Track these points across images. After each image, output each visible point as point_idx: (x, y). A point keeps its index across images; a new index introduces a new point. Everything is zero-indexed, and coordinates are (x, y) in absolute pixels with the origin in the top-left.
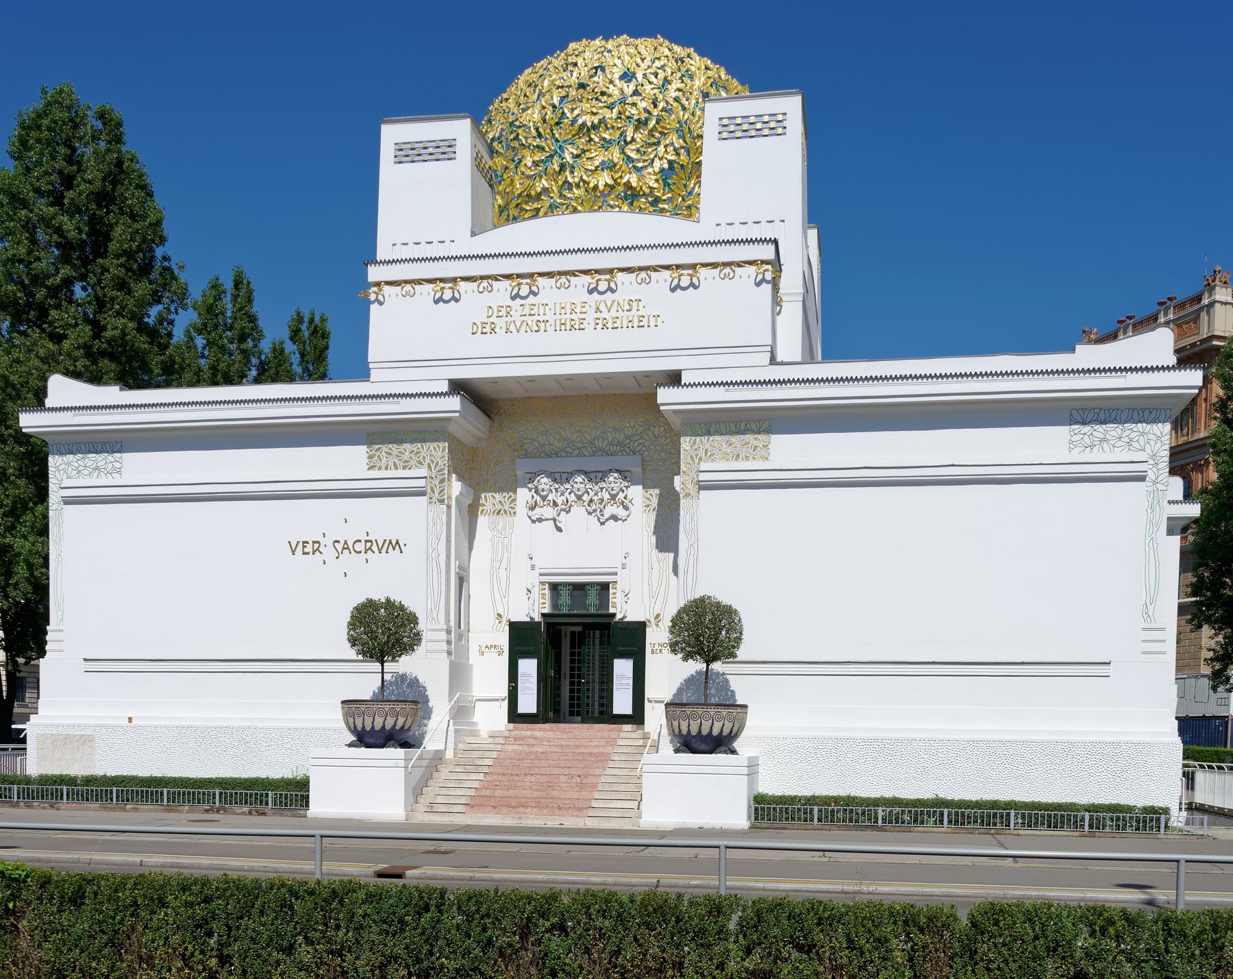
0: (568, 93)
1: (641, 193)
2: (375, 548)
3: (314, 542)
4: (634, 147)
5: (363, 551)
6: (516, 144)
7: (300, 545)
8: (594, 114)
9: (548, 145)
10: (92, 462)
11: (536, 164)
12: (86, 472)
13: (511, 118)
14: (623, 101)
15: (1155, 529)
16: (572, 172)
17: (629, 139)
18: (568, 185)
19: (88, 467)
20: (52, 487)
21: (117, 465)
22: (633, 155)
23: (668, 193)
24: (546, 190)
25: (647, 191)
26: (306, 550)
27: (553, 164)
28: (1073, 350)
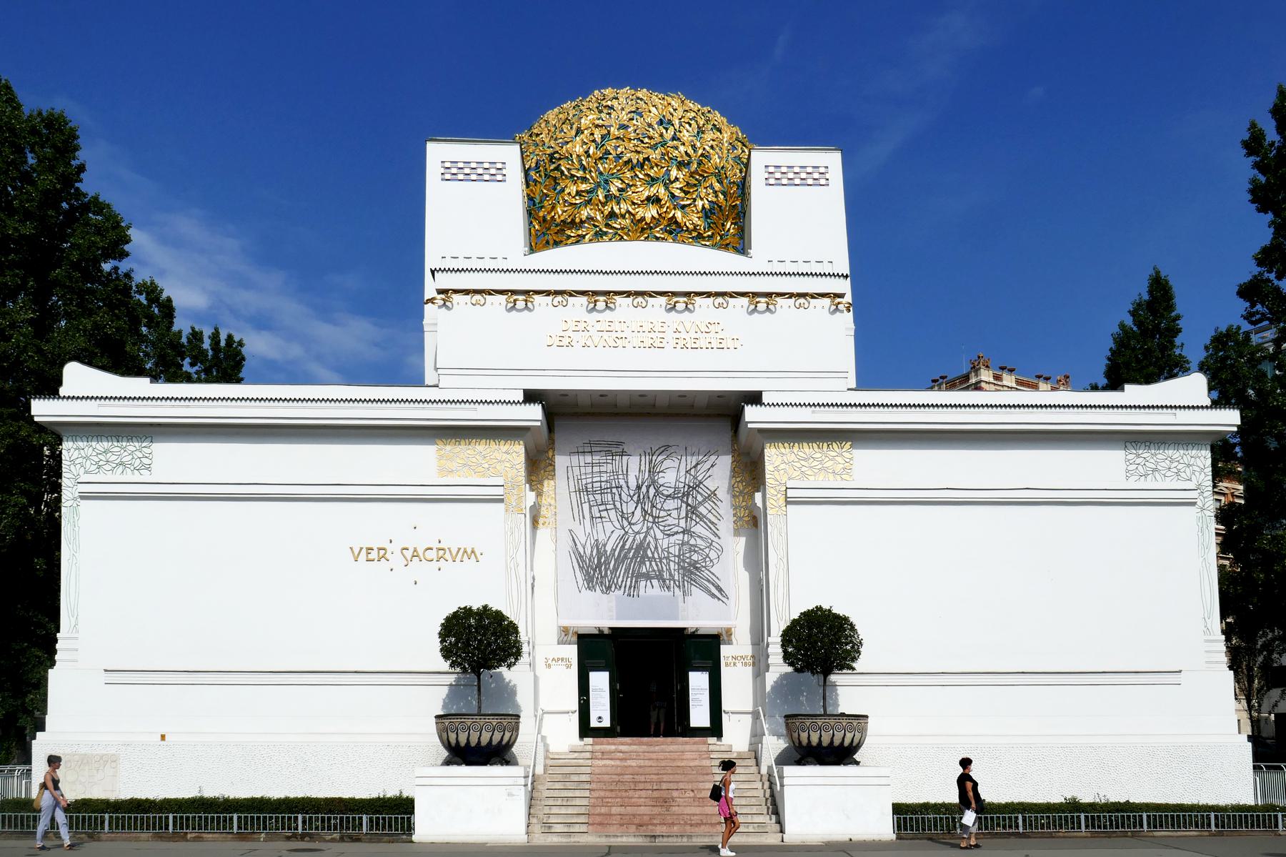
0: (609, 132)
1: (684, 229)
2: (448, 556)
3: (380, 549)
4: (679, 186)
5: (435, 560)
6: (557, 174)
7: (364, 551)
8: (638, 152)
9: (592, 177)
10: (114, 458)
11: (579, 193)
12: (107, 467)
13: (549, 151)
14: (664, 144)
15: (1206, 551)
16: (618, 203)
17: (672, 178)
18: (612, 215)
19: (112, 462)
20: (66, 481)
21: (145, 461)
22: (677, 193)
23: (708, 231)
24: (590, 219)
25: (691, 227)
26: (370, 557)
27: (598, 196)
28: (1123, 390)
